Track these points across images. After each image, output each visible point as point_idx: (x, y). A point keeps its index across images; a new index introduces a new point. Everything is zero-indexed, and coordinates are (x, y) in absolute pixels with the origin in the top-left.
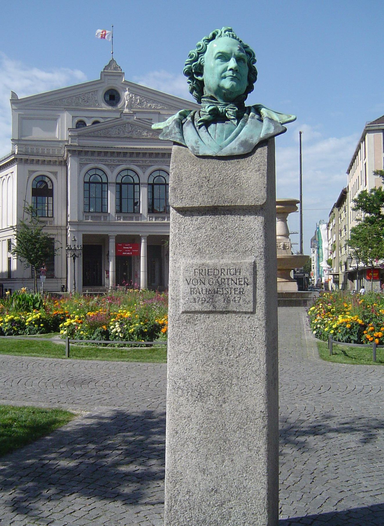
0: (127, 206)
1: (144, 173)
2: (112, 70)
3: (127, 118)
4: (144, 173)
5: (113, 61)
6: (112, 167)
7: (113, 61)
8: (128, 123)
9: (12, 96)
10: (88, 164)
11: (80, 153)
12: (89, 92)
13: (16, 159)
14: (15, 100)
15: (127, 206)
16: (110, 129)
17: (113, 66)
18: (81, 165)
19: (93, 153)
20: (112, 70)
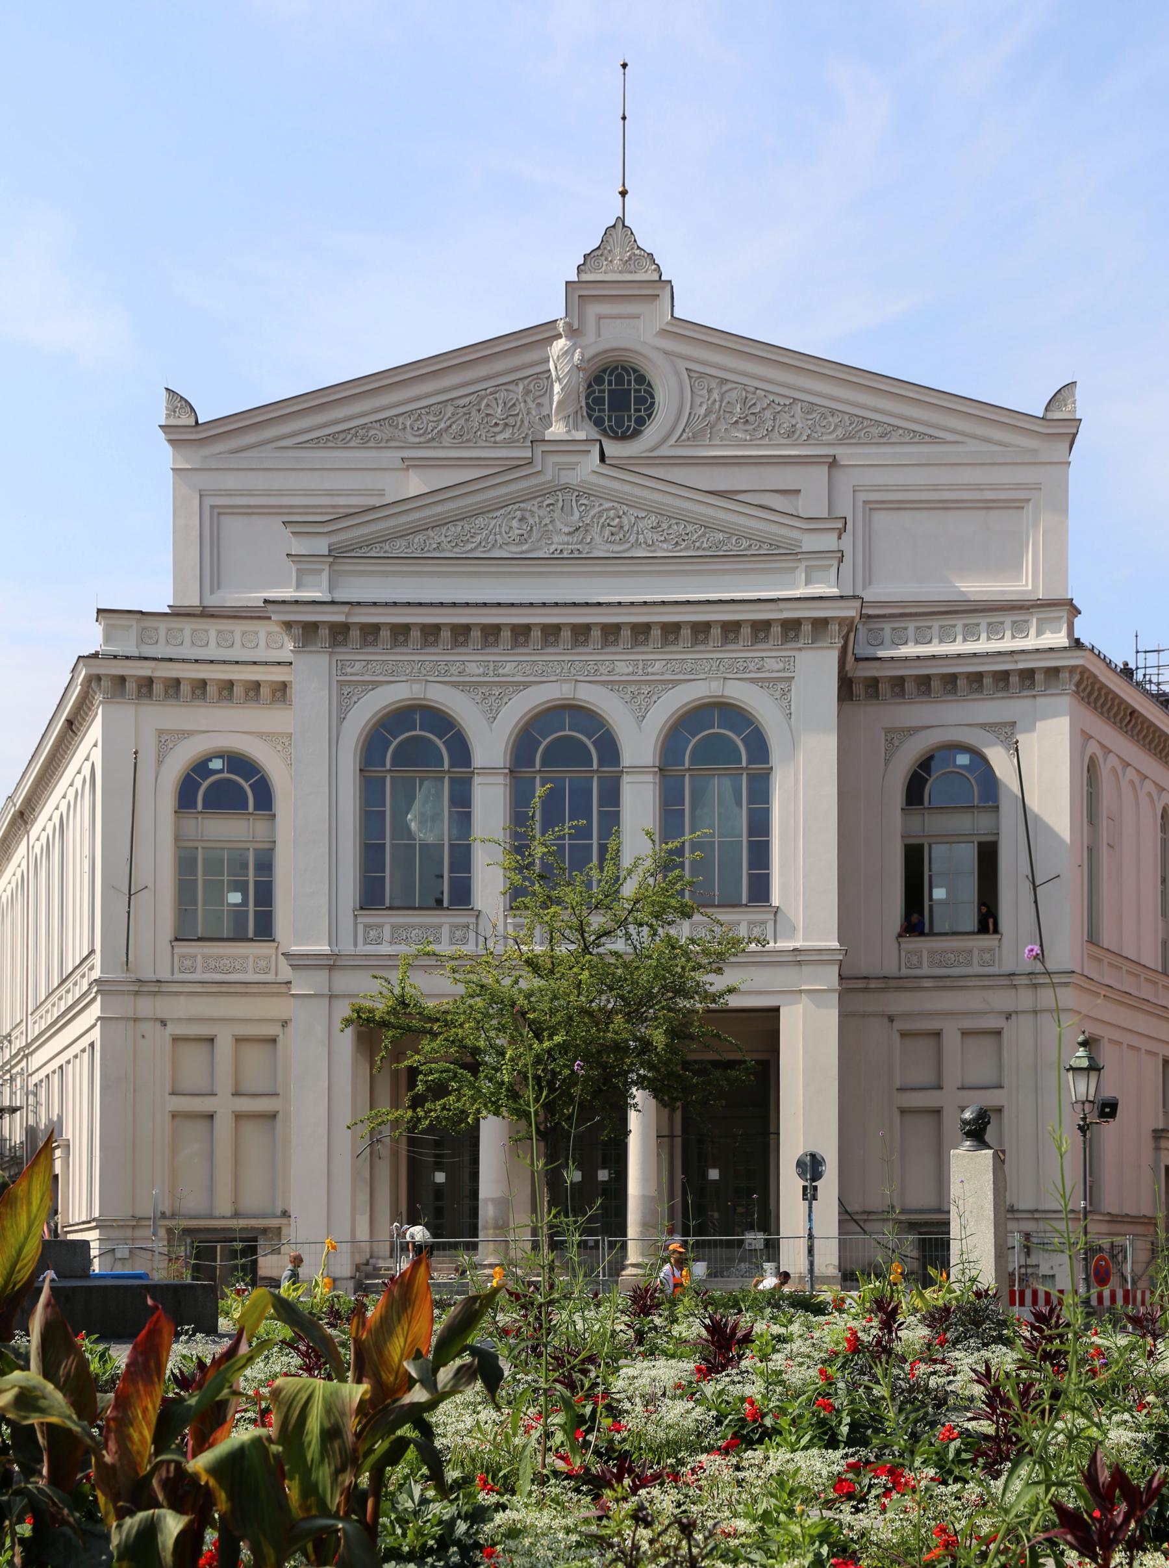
2: (617, 274)
3: (561, 467)
5: (619, 228)
6: (491, 693)
7: (619, 228)
8: (566, 488)
9: (172, 411)
10: (376, 684)
11: (339, 633)
12: (515, 382)
13: (99, 678)
14: (187, 431)
16: (480, 521)
17: (618, 255)
18: (345, 693)
19: (401, 632)
20: (617, 274)
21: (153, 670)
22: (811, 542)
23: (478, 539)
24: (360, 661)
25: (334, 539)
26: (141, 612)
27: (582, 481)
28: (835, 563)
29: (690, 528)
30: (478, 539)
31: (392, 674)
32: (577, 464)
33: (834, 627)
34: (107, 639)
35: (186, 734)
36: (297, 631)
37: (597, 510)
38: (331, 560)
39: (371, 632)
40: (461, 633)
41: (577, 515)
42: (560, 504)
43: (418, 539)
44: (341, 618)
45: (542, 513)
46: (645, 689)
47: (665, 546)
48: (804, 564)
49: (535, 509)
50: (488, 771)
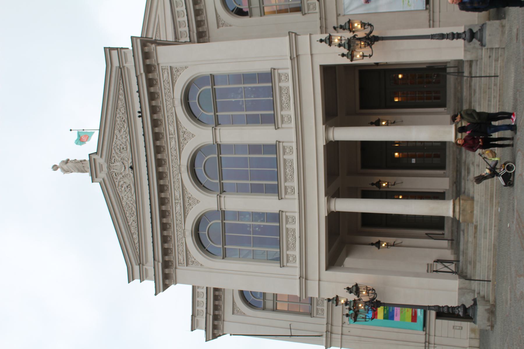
0: (264, 170)
1: (193, 136)
4: (193, 136)
8: (109, 168)
11: (166, 265)
15: (264, 170)
16: (124, 204)
19: (165, 239)
21: (210, 315)
22: (116, 63)
23: (130, 205)
24: (178, 256)
25: (134, 263)
26: (192, 316)
27: (105, 162)
28: (123, 51)
29: (118, 116)
30: (130, 205)
31: (182, 243)
32: (99, 164)
33: (146, 49)
34: (201, 329)
35: (233, 302)
36: (167, 282)
37: (115, 155)
38: (141, 265)
39: (166, 252)
40: (163, 214)
41: (118, 164)
42: (115, 170)
43: (132, 228)
44: (160, 264)
45: (119, 178)
46: (181, 134)
47: (125, 127)
48: (125, 65)
49: (118, 180)
50: (219, 203)
